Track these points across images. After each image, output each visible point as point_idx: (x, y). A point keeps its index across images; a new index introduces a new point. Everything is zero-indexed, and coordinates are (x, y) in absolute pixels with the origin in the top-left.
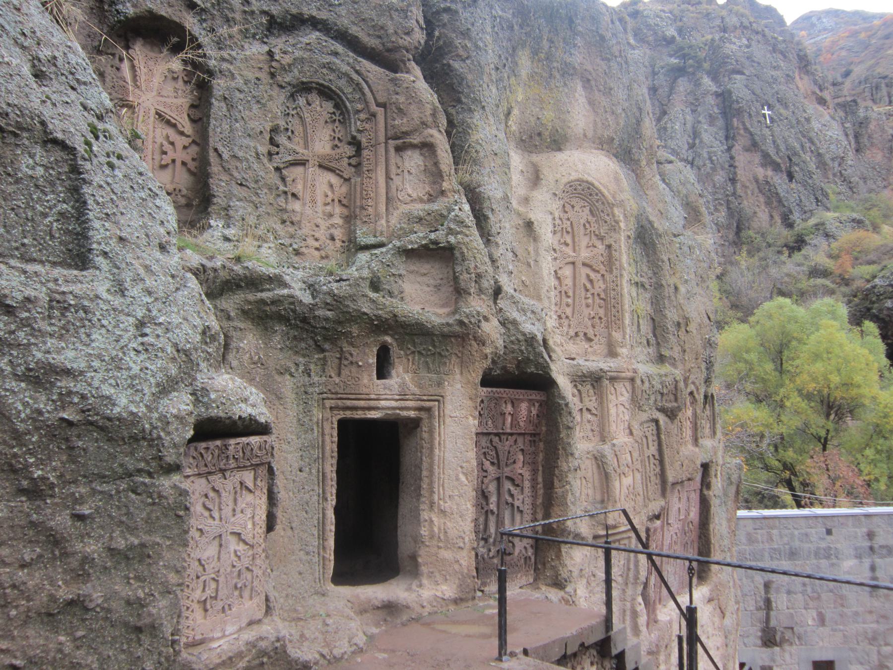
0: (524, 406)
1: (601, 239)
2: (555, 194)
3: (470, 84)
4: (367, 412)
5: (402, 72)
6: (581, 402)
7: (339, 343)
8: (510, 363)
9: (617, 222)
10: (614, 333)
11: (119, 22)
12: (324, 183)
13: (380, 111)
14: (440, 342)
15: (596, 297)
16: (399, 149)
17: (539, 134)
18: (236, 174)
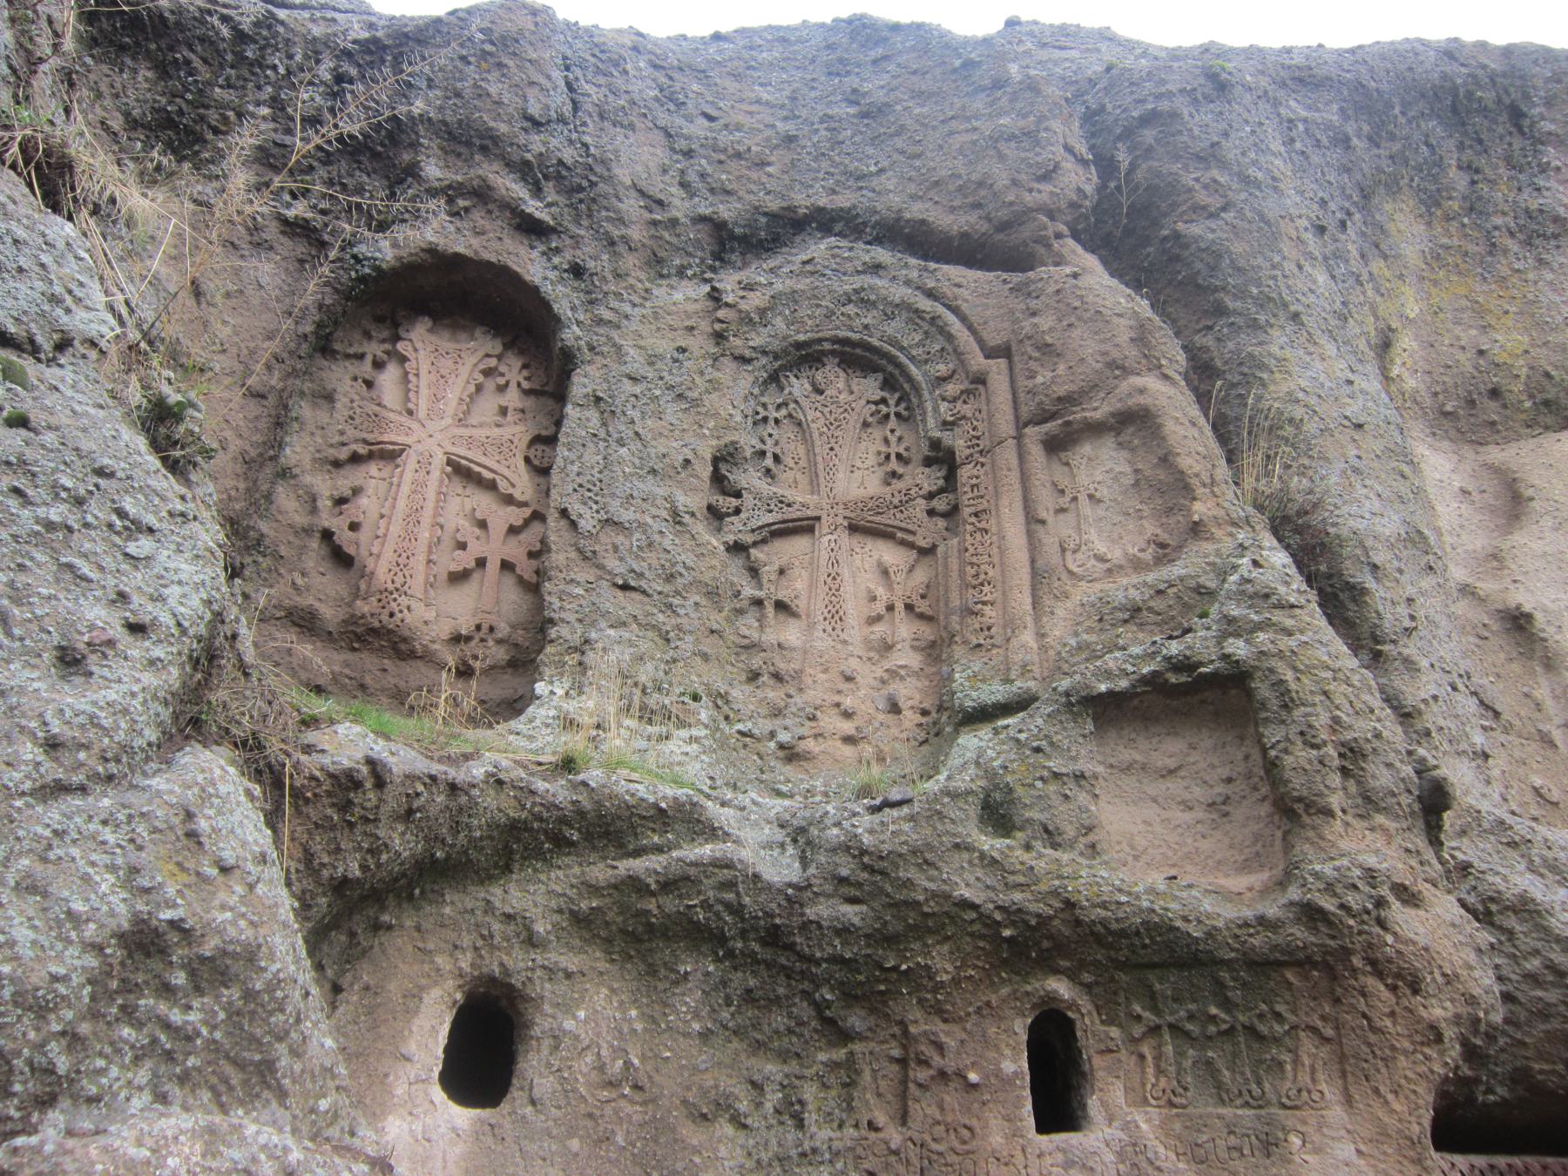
3: (1242, 263)
7: (895, 1008)
8: (1541, 1056)
11: (362, 279)
12: (865, 569)
13: (997, 370)
14: (1245, 984)
16: (1055, 446)
17: (1495, 393)
18: (612, 563)
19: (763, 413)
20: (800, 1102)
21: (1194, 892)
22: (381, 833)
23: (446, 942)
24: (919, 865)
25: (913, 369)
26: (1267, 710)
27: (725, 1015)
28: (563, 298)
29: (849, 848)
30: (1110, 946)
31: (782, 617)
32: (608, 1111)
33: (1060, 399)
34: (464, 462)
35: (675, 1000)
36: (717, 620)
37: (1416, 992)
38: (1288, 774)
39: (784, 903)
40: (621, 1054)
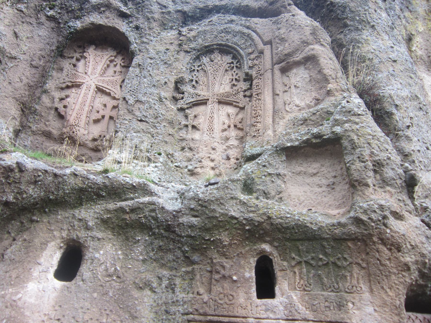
3: (353, 9)
11: (71, 33)
12: (223, 115)
13: (267, 49)
14: (332, 247)
16: (284, 71)
18: (138, 113)
19: (193, 68)
20: (174, 284)
21: (316, 214)
22: (23, 187)
23: (58, 227)
24: (218, 204)
25: (241, 51)
26: (347, 150)
27: (152, 254)
28: (132, 36)
29: (195, 198)
30: (283, 233)
31: (194, 130)
32: (108, 284)
33: (285, 55)
34: (101, 87)
35: (135, 249)
36: (171, 131)
37: (399, 251)
38: (353, 172)
39: (172, 217)
40: (113, 266)
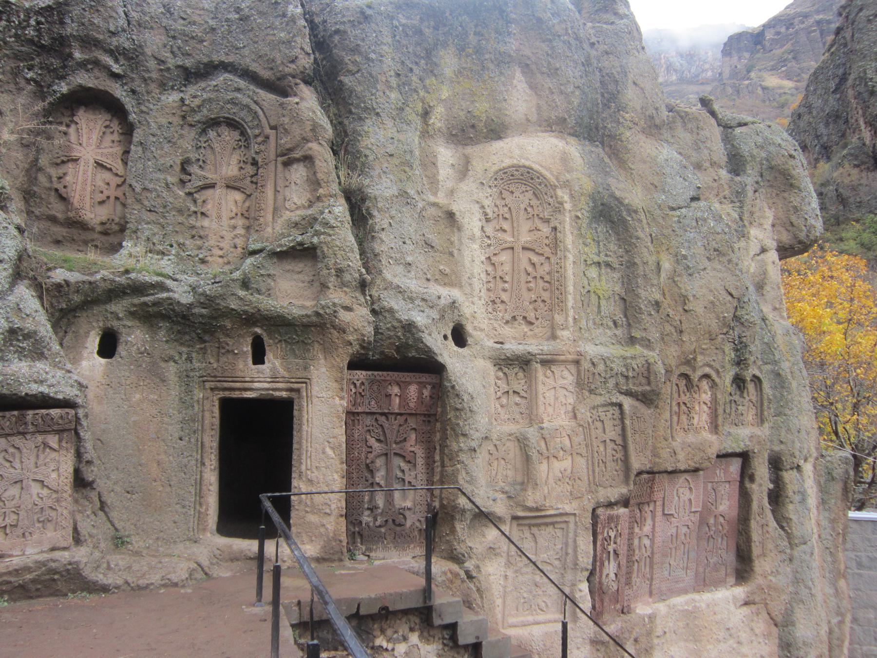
0: (413, 390)
1: (548, 221)
2: (482, 183)
3: (359, 95)
4: (243, 393)
5: (291, 96)
6: (508, 384)
7: (217, 334)
8: (388, 348)
9: (561, 203)
10: (556, 316)
15: (540, 282)
16: (287, 164)
17: (473, 126)
18: (146, 203)
22: (71, 297)
25: (249, 131)
28: (129, 103)
36: (181, 219)
